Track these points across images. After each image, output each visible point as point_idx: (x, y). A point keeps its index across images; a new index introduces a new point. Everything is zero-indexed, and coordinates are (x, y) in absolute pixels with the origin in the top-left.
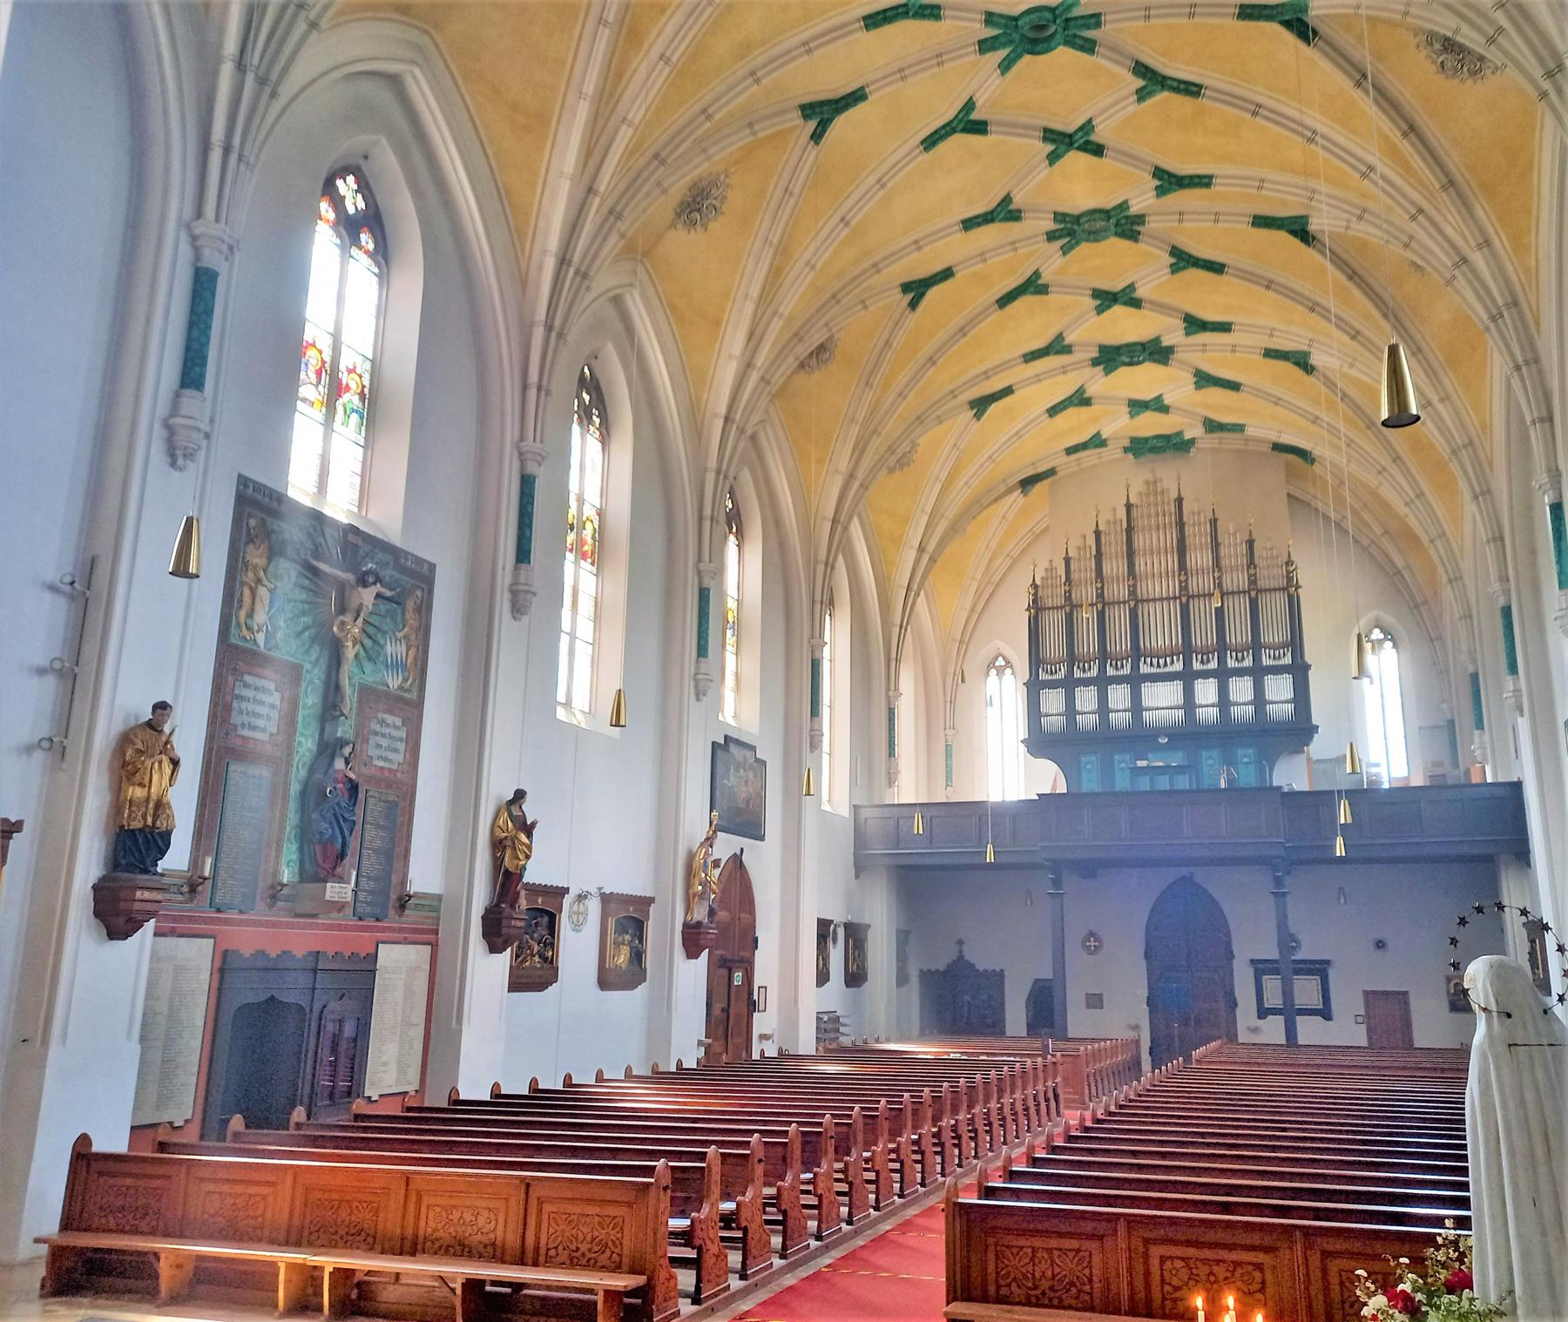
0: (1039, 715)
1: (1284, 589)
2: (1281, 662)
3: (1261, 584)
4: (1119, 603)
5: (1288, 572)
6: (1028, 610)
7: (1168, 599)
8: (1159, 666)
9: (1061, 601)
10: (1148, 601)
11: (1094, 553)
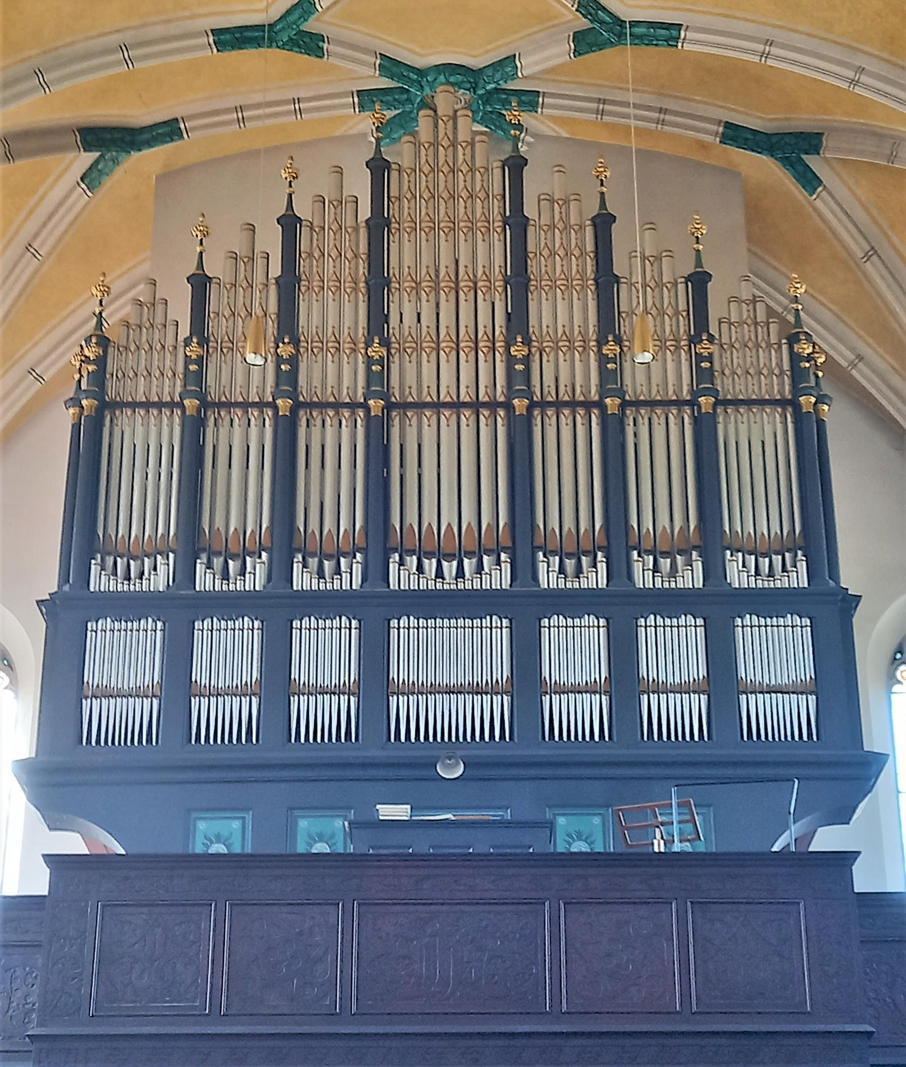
0: (80, 690)
1: (782, 403)
2: (782, 582)
3: (728, 386)
4: (337, 406)
5: (795, 358)
6: (75, 402)
7: (476, 406)
8: (440, 574)
9: (171, 388)
10: (420, 406)
11: (276, 270)
